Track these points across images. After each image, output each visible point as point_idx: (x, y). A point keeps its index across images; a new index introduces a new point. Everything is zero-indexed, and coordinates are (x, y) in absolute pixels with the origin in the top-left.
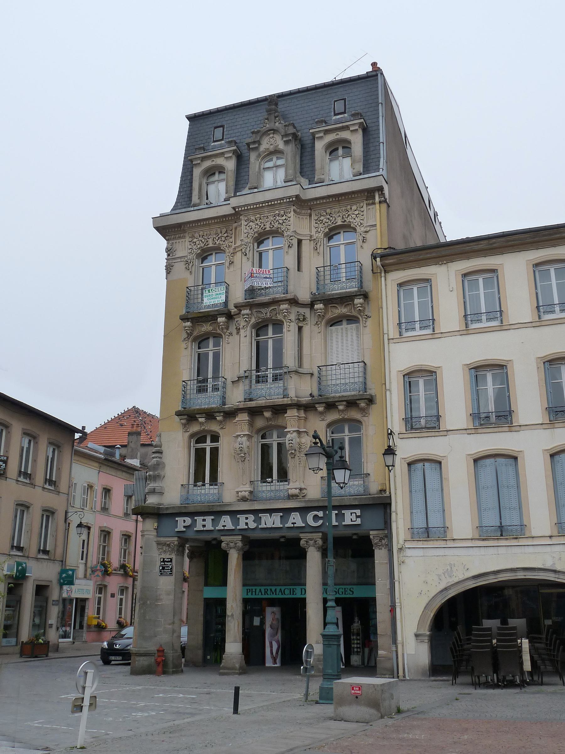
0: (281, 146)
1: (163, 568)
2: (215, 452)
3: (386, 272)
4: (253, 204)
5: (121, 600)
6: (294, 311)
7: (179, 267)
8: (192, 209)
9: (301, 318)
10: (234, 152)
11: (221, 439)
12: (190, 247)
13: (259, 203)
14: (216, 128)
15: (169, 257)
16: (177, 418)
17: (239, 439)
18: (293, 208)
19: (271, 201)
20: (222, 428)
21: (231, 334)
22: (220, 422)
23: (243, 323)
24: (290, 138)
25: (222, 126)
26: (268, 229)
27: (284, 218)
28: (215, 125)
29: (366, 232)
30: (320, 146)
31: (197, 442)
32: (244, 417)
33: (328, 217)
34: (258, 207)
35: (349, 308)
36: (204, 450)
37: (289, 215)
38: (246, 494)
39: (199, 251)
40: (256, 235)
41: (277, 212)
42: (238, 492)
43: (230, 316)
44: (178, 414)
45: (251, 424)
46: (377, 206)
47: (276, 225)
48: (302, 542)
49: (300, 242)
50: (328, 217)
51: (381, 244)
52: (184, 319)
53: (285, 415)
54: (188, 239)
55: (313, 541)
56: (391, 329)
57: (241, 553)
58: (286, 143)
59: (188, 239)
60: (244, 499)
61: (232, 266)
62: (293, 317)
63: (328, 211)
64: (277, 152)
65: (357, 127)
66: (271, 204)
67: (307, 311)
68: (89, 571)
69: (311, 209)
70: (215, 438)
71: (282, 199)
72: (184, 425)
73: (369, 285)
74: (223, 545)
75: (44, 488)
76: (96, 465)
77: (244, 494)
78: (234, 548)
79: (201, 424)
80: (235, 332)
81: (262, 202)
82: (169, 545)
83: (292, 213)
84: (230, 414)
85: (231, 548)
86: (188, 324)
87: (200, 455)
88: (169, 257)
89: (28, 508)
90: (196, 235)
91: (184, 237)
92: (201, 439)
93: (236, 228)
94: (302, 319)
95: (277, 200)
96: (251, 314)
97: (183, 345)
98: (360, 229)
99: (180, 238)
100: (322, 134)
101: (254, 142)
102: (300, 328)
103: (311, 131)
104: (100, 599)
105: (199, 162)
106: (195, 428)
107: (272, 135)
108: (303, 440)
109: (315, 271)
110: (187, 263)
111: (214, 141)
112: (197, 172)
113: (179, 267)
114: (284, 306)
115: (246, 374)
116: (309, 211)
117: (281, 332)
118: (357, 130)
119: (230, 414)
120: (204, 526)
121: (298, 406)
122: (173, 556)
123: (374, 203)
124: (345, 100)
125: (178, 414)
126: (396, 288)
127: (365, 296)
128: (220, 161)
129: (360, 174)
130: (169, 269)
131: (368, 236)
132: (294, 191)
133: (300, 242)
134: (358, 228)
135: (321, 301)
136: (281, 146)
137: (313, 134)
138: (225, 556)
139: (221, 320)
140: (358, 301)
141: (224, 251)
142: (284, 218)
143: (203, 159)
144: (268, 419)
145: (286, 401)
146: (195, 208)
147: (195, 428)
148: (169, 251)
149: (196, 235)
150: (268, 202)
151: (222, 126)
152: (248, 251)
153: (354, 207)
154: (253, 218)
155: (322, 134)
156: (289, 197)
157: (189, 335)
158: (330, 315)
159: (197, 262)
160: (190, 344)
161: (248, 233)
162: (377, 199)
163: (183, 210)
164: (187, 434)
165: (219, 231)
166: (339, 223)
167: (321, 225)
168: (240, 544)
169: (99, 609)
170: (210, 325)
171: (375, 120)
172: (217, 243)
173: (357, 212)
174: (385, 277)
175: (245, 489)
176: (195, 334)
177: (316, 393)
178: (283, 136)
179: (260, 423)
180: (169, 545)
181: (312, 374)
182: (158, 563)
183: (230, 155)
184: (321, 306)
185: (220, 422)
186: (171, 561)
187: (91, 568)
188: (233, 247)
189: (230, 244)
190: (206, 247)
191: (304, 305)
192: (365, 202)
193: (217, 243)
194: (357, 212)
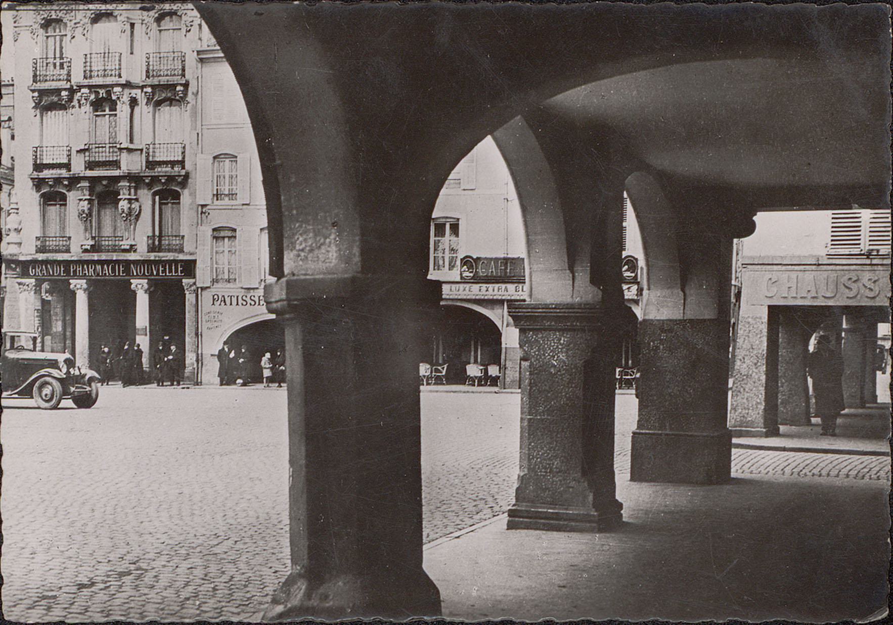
20: (68, 191)
21: (73, 107)
38: (89, 247)
39: (43, 22)
40: (93, 16)
42: (82, 246)
45: (91, 190)
48: (133, 286)
49: (132, 25)
53: (119, 185)
55: (141, 286)
61: (73, 40)
62: (126, 98)
74: (72, 286)
77: (86, 247)
78: (81, 288)
85: (78, 289)
86: (36, 94)
94: (133, 102)
108: (133, 206)
109: (144, 56)
115: (86, 147)
117: (115, 110)
133: (132, 25)
138: (74, 294)
141: (66, 24)
159: (42, 31)
168: (85, 286)
170: (55, 97)
172: (60, 15)
180: (28, 285)
181: (141, 150)
188: (74, 21)
189: (71, 18)
190: (49, 18)
193: (60, 15)
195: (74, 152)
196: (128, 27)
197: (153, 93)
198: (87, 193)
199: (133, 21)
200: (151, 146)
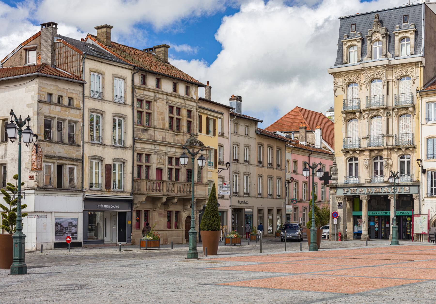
0: (381, 39)
1: (339, 206)
2: (356, 164)
3: (421, 97)
4: (369, 67)
5: (304, 214)
6: (386, 111)
7: (339, 90)
8: (344, 65)
9: (389, 115)
10: (360, 39)
11: (358, 160)
12: (343, 81)
13: (371, 67)
14: (352, 25)
15: (335, 85)
16: (342, 152)
17: (366, 161)
18: (386, 69)
19: (377, 66)
22: (358, 154)
23: (366, 116)
24: (384, 35)
25: (355, 24)
26: (375, 77)
27: (382, 73)
28: (352, 23)
29: (415, 79)
30: (397, 39)
31: (349, 161)
32: (367, 153)
33: (400, 72)
34: (371, 68)
35: (407, 111)
36: (352, 164)
37: (384, 72)
38: (369, 181)
40: (371, 80)
41: (379, 70)
43: (361, 112)
44: (342, 151)
45: (370, 155)
46: (419, 69)
47: (379, 76)
50: (400, 72)
51: (420, 85)
52: (343, 113)
54: (342, 78)
56: (424, 122)
57: (367, 201)
58: (383, 37)
59: (342, 78)
60: (368, 182)
61: (361, 91)
63: (400, 69)
64: (378, 40)
65: (412, 32)
66: (376, 67)
67: (391, 111)
68: (290, 201)
69: (393, 68)
70: (356, 159)
71: (381, 65)
72: (344, 155)
73: (416, 102)
74: (361, 198)
75: (277, 169)
76: (290, 150)
77: (367, 180)
78: (365, 199)
79: (351, 154)
80: (363, 118)
81: (373, 67)
82: (341, 198)
83: (385, 71)
84: (362, 151)
86: (344, 115)
87: (351, 165)
88: (335, 85)
89: (272, 178)
90: (346, 76)
91: (341, 77)
92: (351, 159)
93: (362, 74)
95: (379, 66)
96: (369, 113)
97: (343, 123)
98: (412, 78)
99: (339, 77)
100: (397, 34)
101: (369, 37)
102: (388, 118)
103: (393, 32)
104: (295, 213)
105: (346, 43)
106: (349, 156)
107: (376, 33)
110: (342, 88)
111: (352, 31)
112: (345, 47)
113: (339, 90)
114: (382, 111)
116: (392, 69)
118: (412, 33)
119: (362, 151)
120: (353, 192)
121: (388, 149)
122: (343, 202)
123: (418, 67)
124: (408, 15)
125: (342, 151)
126: (425, 104)
127: (414, 107)
128: (355, 43)
129: (413, 54)
130: (335, 91)
131: (416, 81)
132: (386, 62)
133: (388, 82)
134: (411, 77)
135: (396, 108)
136: (381, 39)
137: (394, 34)
139: (358, 114)
140: (411, 109)
142: (382, 73)
143: (347, 41)
144: (376, 154)
145: (383, 147)
146: (346, 65)
147: (349, 156)
148: (335, 83)
149: (346, 76)
150: (375, 66)
151: (355, 24)
152: (367, 86)
153: (410, 68)
154: (369, 72)
155: (397, 34)
156: (384, 65)
157: (345, 119)
158: (400, 114)
160: (345, 122)
161: (367, 79)
162: (419, 66)
163: (340, 66)
164: (345, 158)
165: (355, 75)
166: (404, 75)
167: (397, 75)
169: (295, 218)
171: (420, 27)
173: (411, 71)
174: (421, 100)
175: (368, 179)
176: (347, 118)
177: (394, 144)
178: (381, 35)
179: (373, 154)
180: (341, 198)
182: (337, 204)
183: (359, 40)
184: (396, 110)
185: (358, 154)
186: (342, 203)
187: (291, 200)
188: (361, 83)
191: (390, 110)
192: (415, 66)
194: (411, 71)
195: (362, 139)
196: (386, 84)
197: (398, 112)
198: (368, 156)
199: (388, 81)
200: (397, 135)
